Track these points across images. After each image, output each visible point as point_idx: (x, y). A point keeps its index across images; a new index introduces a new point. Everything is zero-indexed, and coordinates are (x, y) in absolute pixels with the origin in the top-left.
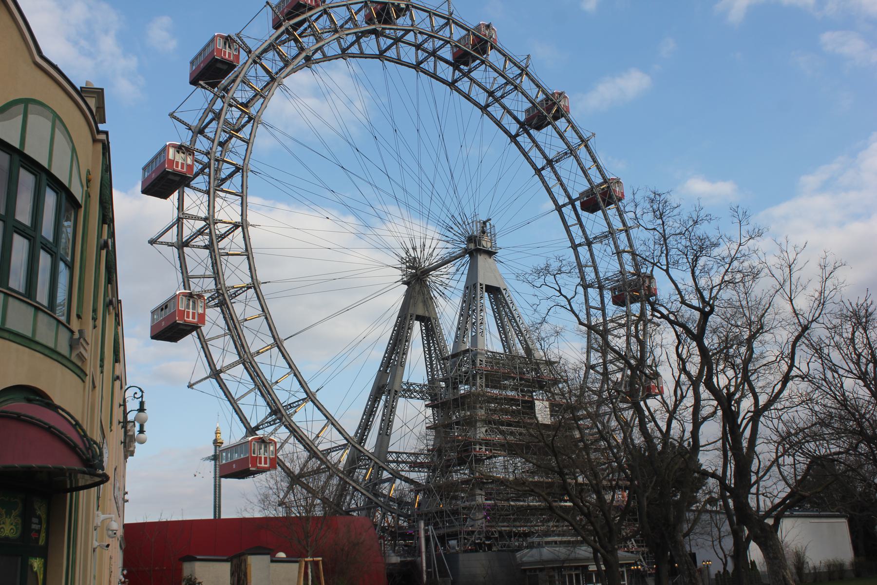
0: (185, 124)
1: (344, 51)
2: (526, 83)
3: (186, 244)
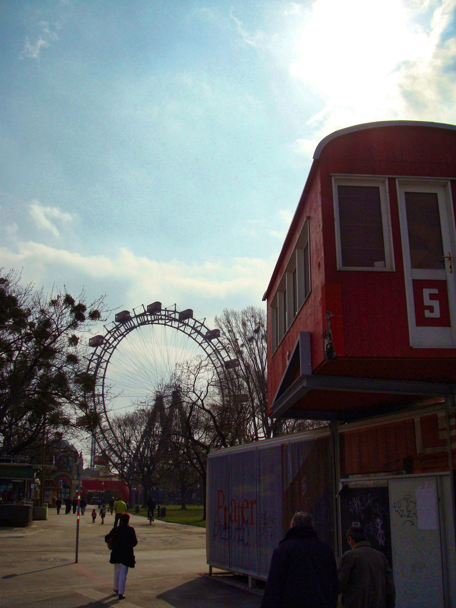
0: (107, 329)
1: (165, 323)
3: (92, 361)
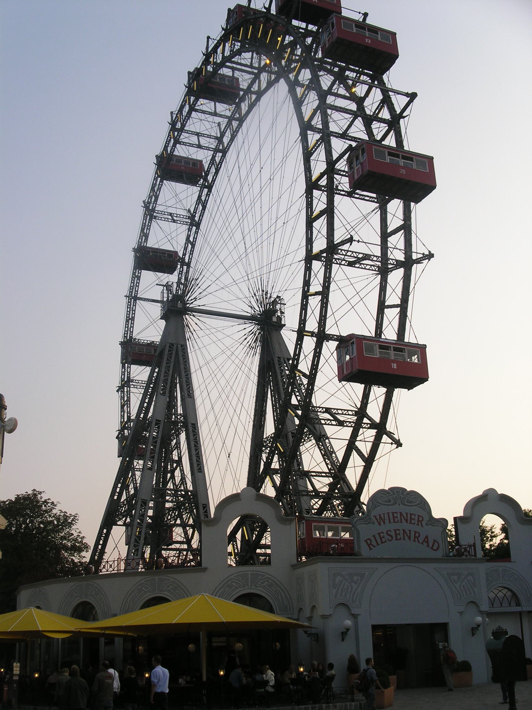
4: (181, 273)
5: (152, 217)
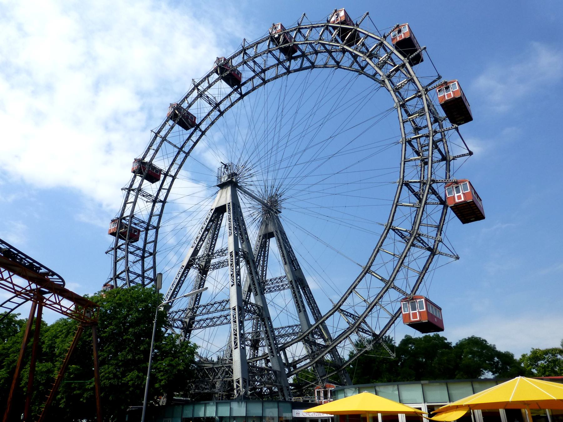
2: (136, 186)
4: (192, 133)
5: (200, 95)
